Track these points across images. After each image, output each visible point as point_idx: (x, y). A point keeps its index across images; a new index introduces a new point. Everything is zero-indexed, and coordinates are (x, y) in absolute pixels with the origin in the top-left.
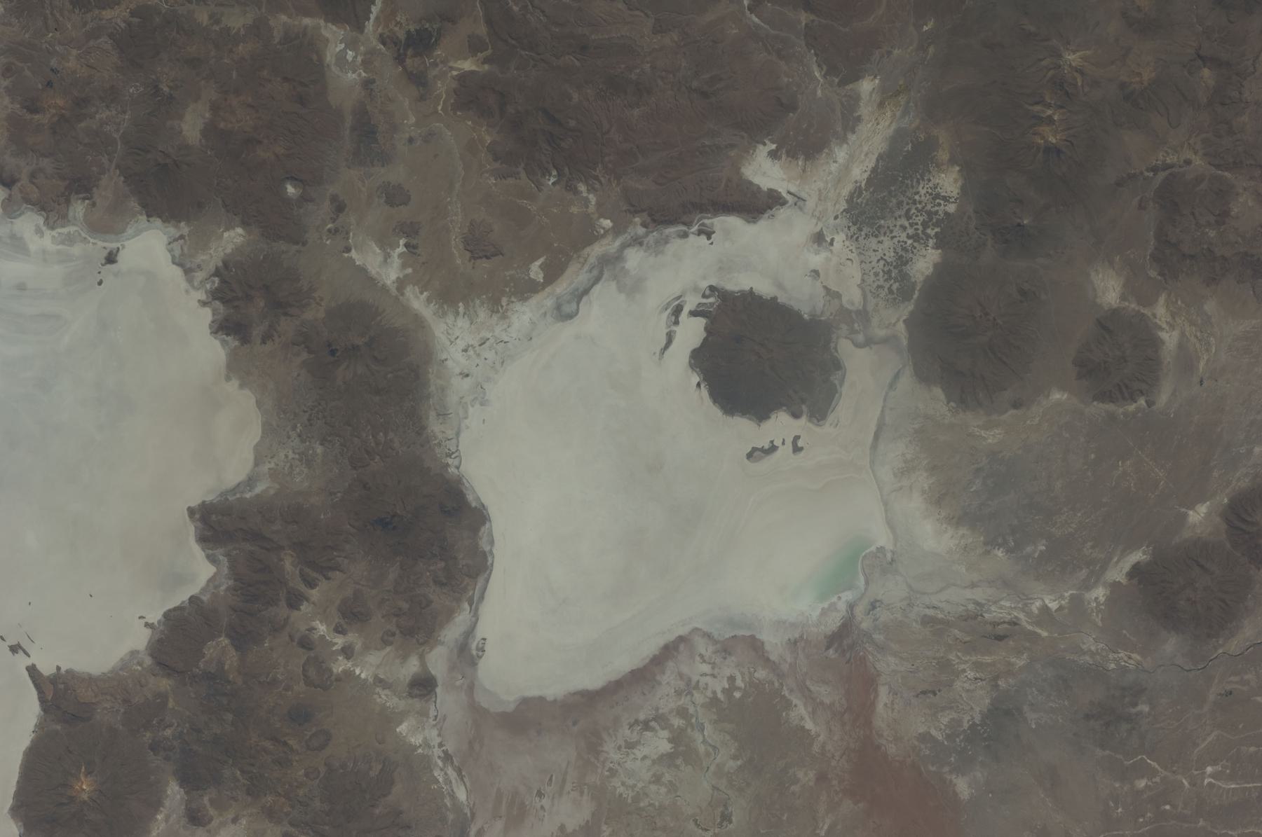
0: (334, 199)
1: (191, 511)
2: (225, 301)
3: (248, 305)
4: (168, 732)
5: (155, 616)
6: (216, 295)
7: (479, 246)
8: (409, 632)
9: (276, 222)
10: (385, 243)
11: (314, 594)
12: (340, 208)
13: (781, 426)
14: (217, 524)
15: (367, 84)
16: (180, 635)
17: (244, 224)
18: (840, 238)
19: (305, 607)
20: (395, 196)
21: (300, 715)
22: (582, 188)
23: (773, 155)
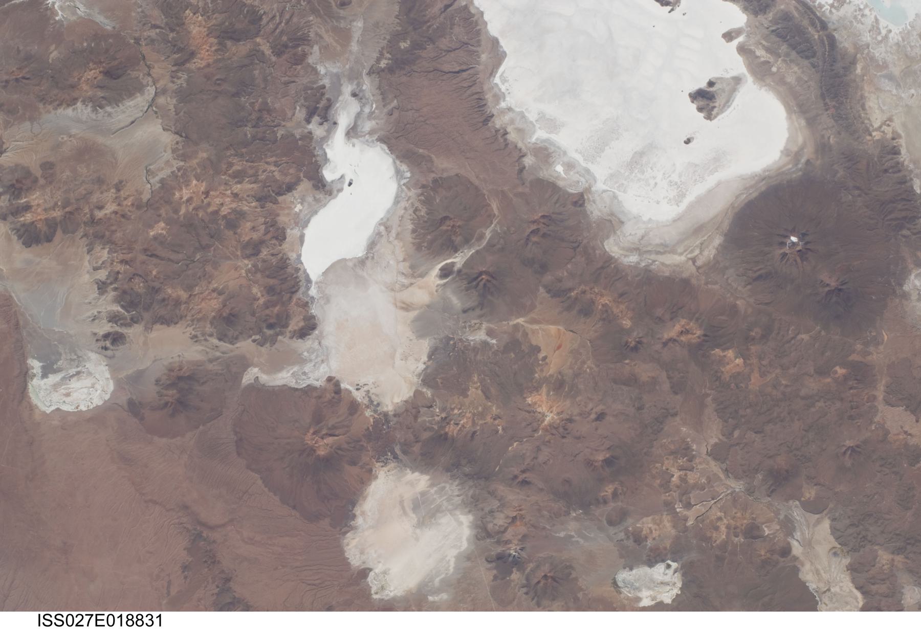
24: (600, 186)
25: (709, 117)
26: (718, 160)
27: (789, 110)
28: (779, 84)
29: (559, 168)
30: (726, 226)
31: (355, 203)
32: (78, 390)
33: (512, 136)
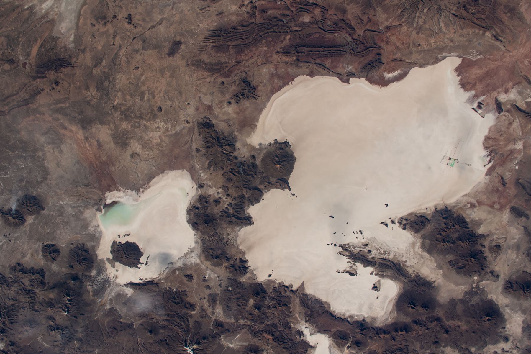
0: (221, 287)
1: (253, 224)
2: (245, 267)
3: (241, 266)
4: (260, 176)
5: (262, 201)
6: (247, 268)
7: (190, 277)
8: (205, 198)
9: (234, 282)
10: (210, 278)
11: (226, 206)
12: (220, 285)
13: (123, 241)
14: (248, 221)
15: (214, 309)
16: (256, 196)
17: (241, 282)
18: (112, 278)
19: (228, 203)
20: (208, 287)
21: (229, 180)
22: (168, 289)
23: (127, 294)
24: (366, 316)
25: (378, 291)
26: (386, 297)
27: (392, 280)
28: (388, 277)
29: (356, 317)
30: (395, 308)
33: (342, 317)
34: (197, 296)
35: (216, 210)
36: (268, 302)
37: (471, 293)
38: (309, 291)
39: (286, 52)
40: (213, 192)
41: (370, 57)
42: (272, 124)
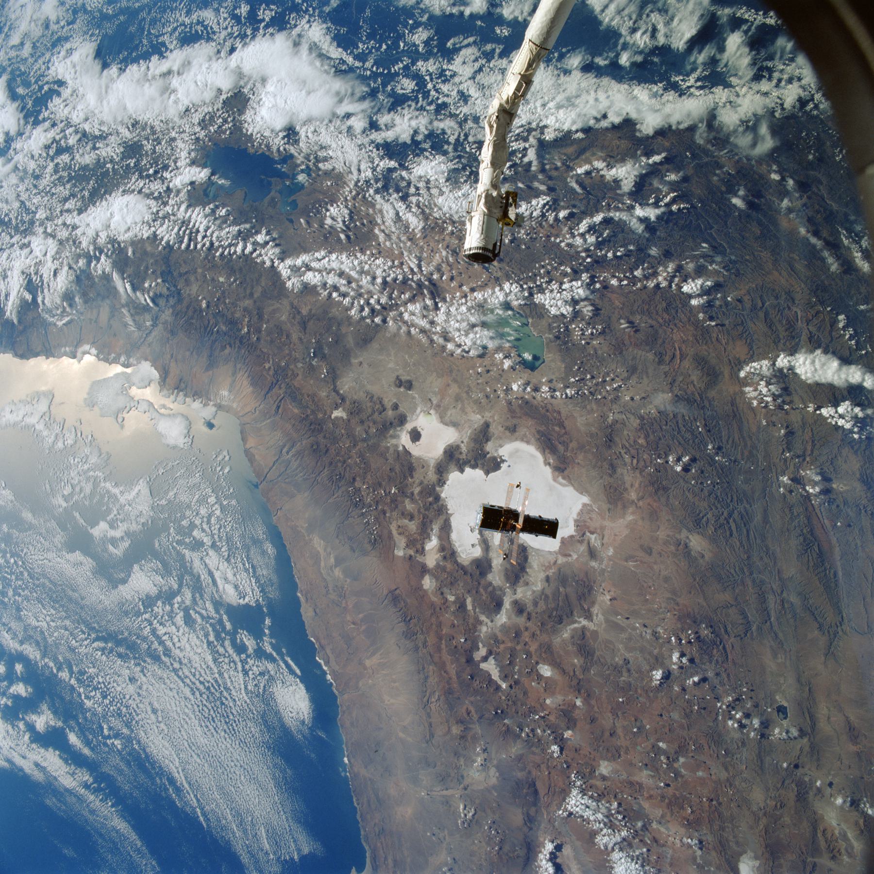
3: (442, 482)
7: (423, 467)
9: (434, 486)
13: (419, 430)
14: (462, 471)
16: (474, 467)
31: (433, 544)
32: (400, 553)
34: (418, 476)
35: (457, 456)
36: (435, 506)
37: (501, 589)
38: (452, 519)
39: (538, 432)
40: (464, 449)
41: (562, 466)
42: (507, 450)
